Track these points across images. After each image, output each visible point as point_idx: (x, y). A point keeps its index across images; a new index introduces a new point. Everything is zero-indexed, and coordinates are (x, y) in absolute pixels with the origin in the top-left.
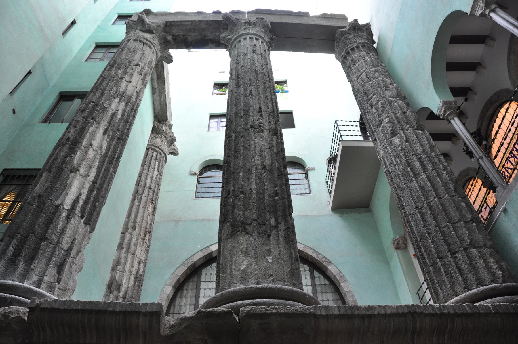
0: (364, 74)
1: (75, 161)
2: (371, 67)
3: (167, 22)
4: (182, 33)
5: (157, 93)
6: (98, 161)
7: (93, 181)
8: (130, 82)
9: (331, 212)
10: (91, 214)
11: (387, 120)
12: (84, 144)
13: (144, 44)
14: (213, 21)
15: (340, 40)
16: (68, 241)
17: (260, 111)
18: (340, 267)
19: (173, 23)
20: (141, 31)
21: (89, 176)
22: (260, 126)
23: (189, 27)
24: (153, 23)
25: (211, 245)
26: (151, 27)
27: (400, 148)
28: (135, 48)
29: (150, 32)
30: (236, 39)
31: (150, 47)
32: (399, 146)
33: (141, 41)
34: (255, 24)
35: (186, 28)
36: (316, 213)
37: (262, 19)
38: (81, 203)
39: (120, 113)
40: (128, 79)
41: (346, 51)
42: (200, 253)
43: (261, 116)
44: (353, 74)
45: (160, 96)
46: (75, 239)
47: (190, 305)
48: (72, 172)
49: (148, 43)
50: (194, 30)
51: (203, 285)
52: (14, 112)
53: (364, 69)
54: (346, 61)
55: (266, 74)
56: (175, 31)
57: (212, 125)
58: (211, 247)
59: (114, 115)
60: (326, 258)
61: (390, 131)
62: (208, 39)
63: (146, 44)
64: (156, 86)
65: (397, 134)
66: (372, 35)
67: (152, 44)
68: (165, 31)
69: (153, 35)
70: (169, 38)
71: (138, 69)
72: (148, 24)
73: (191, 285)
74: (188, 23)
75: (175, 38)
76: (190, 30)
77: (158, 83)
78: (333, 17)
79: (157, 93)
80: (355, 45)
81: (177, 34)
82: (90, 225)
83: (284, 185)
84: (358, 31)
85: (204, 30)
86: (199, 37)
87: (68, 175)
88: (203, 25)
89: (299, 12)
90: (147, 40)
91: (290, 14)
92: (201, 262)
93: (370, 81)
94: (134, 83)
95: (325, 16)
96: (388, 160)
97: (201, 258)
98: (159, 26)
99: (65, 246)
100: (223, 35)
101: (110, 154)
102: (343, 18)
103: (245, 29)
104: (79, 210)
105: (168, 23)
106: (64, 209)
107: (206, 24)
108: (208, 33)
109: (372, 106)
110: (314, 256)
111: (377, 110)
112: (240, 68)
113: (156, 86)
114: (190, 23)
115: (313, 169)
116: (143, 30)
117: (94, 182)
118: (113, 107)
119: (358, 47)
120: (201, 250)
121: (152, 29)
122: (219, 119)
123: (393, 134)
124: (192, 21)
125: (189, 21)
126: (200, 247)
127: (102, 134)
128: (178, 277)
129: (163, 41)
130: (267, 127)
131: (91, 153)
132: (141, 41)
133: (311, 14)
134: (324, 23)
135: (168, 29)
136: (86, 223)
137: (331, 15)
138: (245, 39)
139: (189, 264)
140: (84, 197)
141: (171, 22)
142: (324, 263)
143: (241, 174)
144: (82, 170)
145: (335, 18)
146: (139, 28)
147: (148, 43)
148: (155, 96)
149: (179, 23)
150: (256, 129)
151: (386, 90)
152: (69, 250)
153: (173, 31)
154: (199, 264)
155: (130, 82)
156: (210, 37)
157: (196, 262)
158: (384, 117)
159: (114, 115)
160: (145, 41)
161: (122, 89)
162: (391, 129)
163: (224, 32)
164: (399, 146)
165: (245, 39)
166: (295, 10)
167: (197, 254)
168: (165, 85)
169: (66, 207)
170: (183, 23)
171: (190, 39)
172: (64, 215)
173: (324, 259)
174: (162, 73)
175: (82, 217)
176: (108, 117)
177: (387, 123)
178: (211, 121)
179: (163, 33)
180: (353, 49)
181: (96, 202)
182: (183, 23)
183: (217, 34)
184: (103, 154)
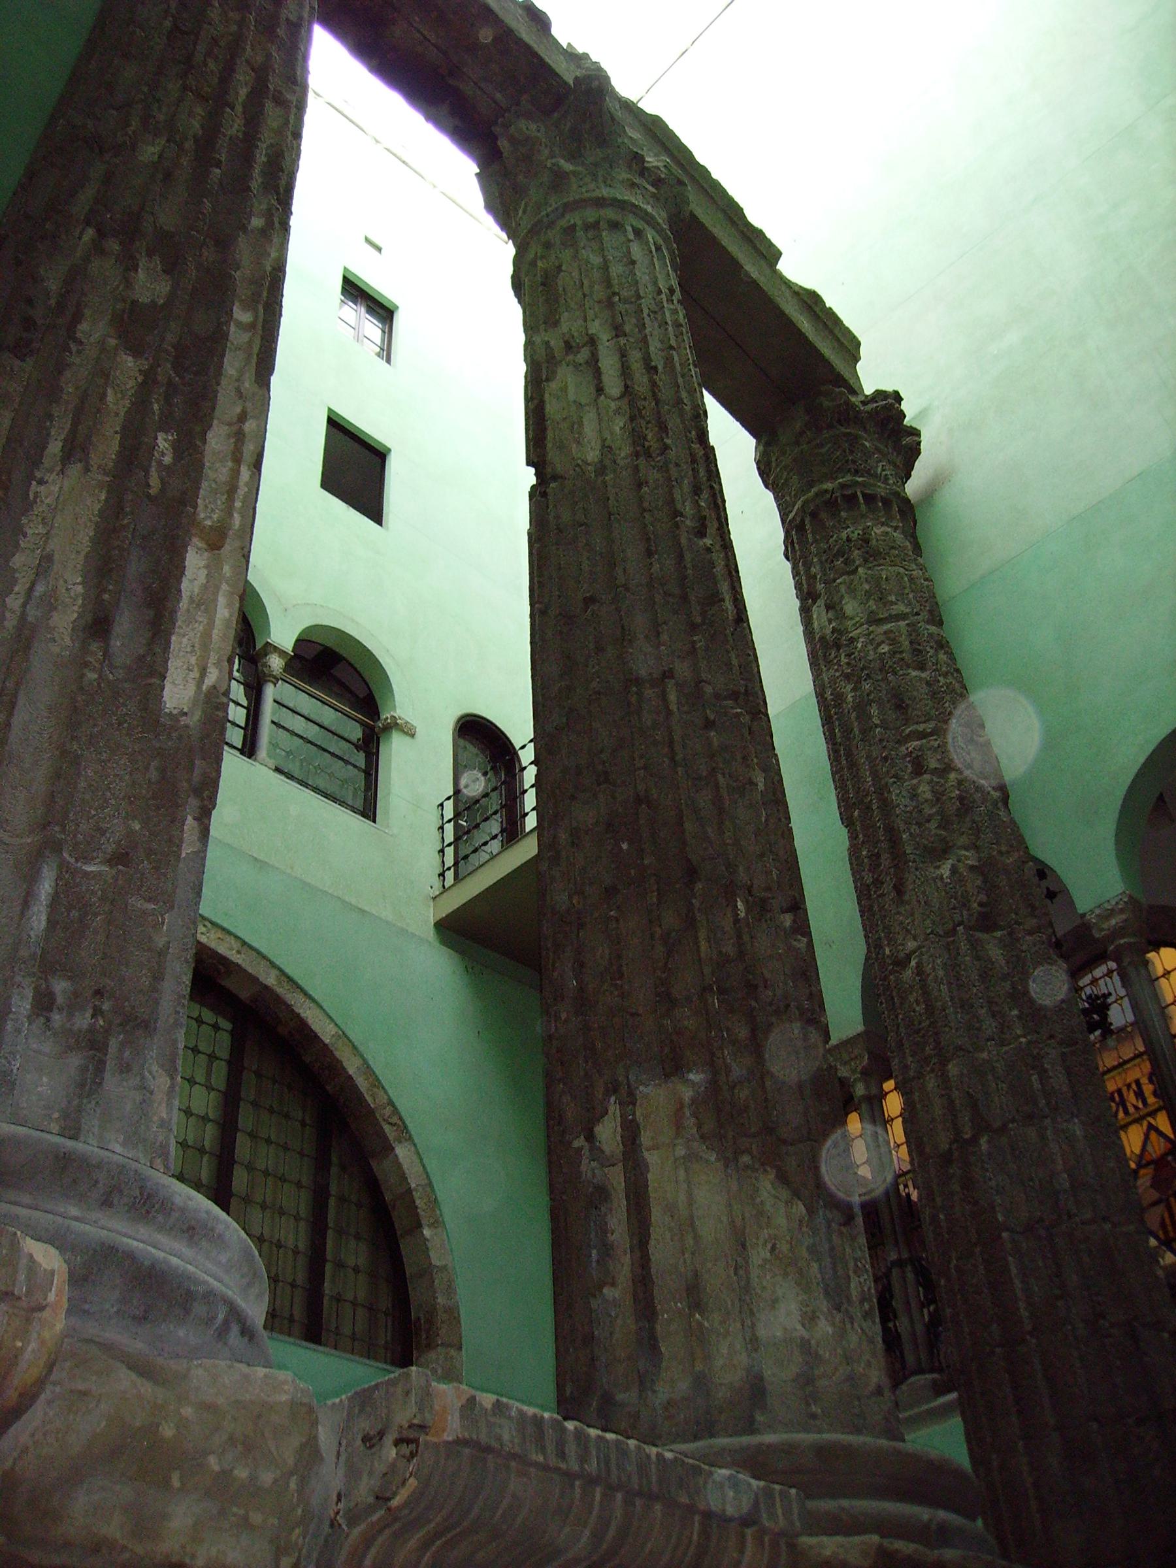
0: (902, 624)
2: (924, 615)
9: (430, 933)
11: (971, 858)
15: (830, 426)
18: (432, 1165)
27: (1007, 985)
30: (600, 202)
32: (1005, 977)
34: (658, 182)
36: (387, 914)
37: (680, 183)
41: (843, 486)
44: (852, 591)
53: (901, 608)
54: (823, 515)
60: (396, 1111)
61: (981, 904)
65: (994, 927)
66: (908, 476)
78: (828, 321)
80: (881, 490)
84: (889, 437)
89: (760, 233)
91: (732, 212)
93: (922, 667)
95: (811, 301)
96: (952, 999)
100: (529, 128)
102: (850, 347)
103: (633, 185)
107: (497, 40)
109: (919, 768)
110: (362, 1083)
111: (938, 797)
112: (635, 356)
115: (410, 733)
119: (886, 502)
123: (987, 922)
133: (782, 266)
134: (805, 325)
137: (830, 313)
138: (638, 233)
142: (387, 1128)
143: (739, 904)
145: (831, 332)
151: (971, 741)
156: (468, 89)
158: (963, 840)
162: (982, 897)
163: (529, 116)
164: (1005, 977)
165: (638, 233)
166: (754, 217)
173: (389, 1109)
177: (972, 868)
180: (870, 499)
183: (498, 96)
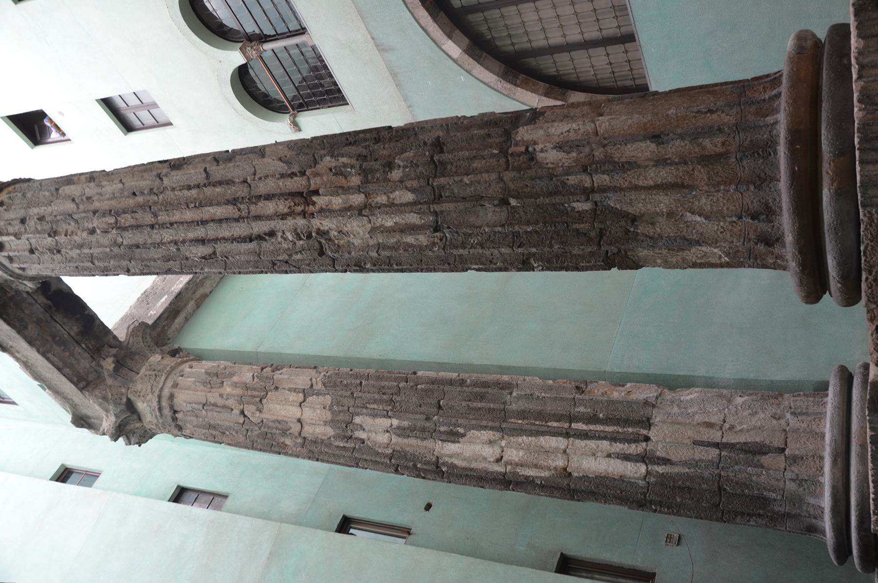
1: (545, 474)
3: (81, 390)
4: (78, 349)
5: (201, 291)
6: (520, 439)
7: (564, 437)
8: (299, 421)
10: (626, 422)
12: (502, 470)
13: (175, 412)
14: (9, 324)
16: (702, 451)
17: (260, 238)
19: (75, 379)
20: (140, 419)
21: (565, 451)
22: (309, 236)
23: (58, 349)
24: (107, 411)
25: (450, 57)
26: (122, 411)
28: (204, 427)
29: (130, 406)
31: (172, 397)
33: (174, 419)
35: (64, 351)
38: (618, 447)
39: (385, 422)
40: (296, 428)
42: (475, 72)
43: (272, 234)
45: (202, 282)
46: (696, 443)
47: (590, 57)
48: (570, 474)
49: (165, 403)
50: (54, 337)
51: (539, 41)
52: (428, 507)
55: (112, 220)
56: (85, 363)
57: (148, 119)
58: (455, 56)
59: (402, 432)
62: (48, 298)
63: (172, 407)
64: (192, 304)
67: (160, 397)
68: (100, 379)
69: (132, 398)
70: (109, 364)
71: (249, 410)
72: (116, 416)
73: (547, 64)
74: (55, 359)
75: (97, 352)
76: (62, 343)
77: (185, 306)
79: (201, 291)
81: (86, 355)
82: (648, 419)
83: (461, 181)
85: (39, 322)
86: (58, 317)
87: (580, 478)
88: (32, 330)
90: (160, 409)
92: (491, 61)
94: (294, 412)
97: (487, 68)
98: (105, 398)
99: (714, 453)
101: (490, 424)
104: (633, 446)
105: (81, 385)
106: (648, 473)
107: (26, 328)
108: (38, 310)
113: (192, 304)
114: (50, 355)
116: (135, 417)
117: (567, 435)
118: (383, 438)
120: (469, 72)
121: (123, 407)
122: (123, 112)
124: (44, 355)
125: (48, 359)
126: (463, 77)
127: (457, 445)
128: (543, 98)
129: (124, 371)
130: (301, 222)
131: (513, 455)
132: (174, 419)
135: (91, 377)
136: (647, 423)
139: (508, 86)
140: (605, 444)
141: (76, 384)
144: (560, 463)
146: (138, 425)
147: (165, 403)
148: (207, 291)
149: (67, 370)
150: (320, 243)
152: (717, 445)
153: (88, 366)
154: (496, 64)
155: (299, 421)
157: (498, 75)
159: (402, 432)
160: (167, 411)
161: (330, 431)
167: (481, 77)
168: (179, 294)
169: (643, 468)
170: (60, 365)
171: (75, 328)
172: (660, 469)
174: (166, 315)
175: (647, 439)
176: (412, 441)
178: (137, 123)
179: (110, 381)
181: (598, 418)
182: (60, 365)
184: (498, 435)
